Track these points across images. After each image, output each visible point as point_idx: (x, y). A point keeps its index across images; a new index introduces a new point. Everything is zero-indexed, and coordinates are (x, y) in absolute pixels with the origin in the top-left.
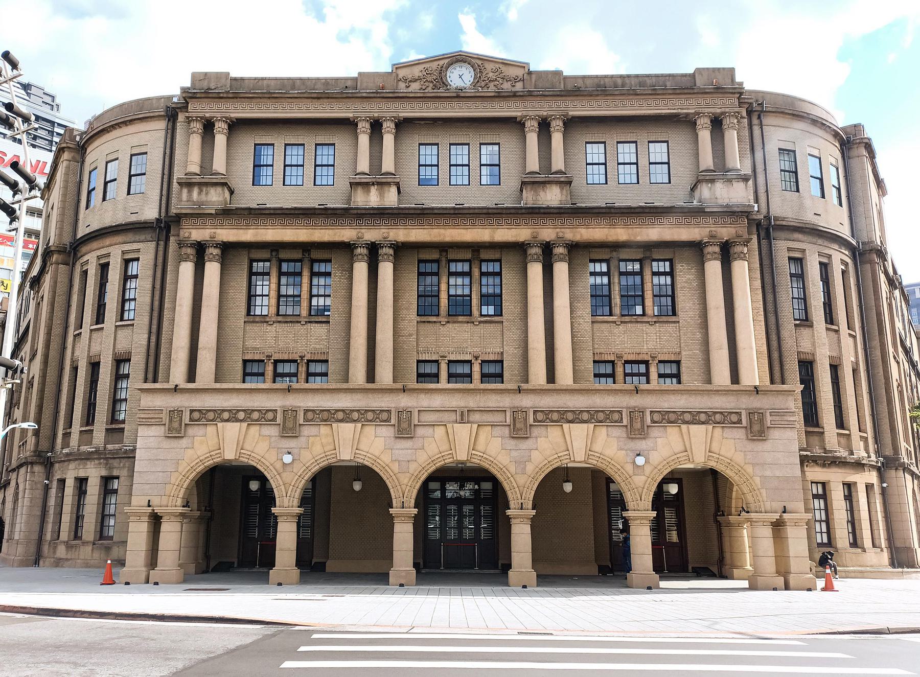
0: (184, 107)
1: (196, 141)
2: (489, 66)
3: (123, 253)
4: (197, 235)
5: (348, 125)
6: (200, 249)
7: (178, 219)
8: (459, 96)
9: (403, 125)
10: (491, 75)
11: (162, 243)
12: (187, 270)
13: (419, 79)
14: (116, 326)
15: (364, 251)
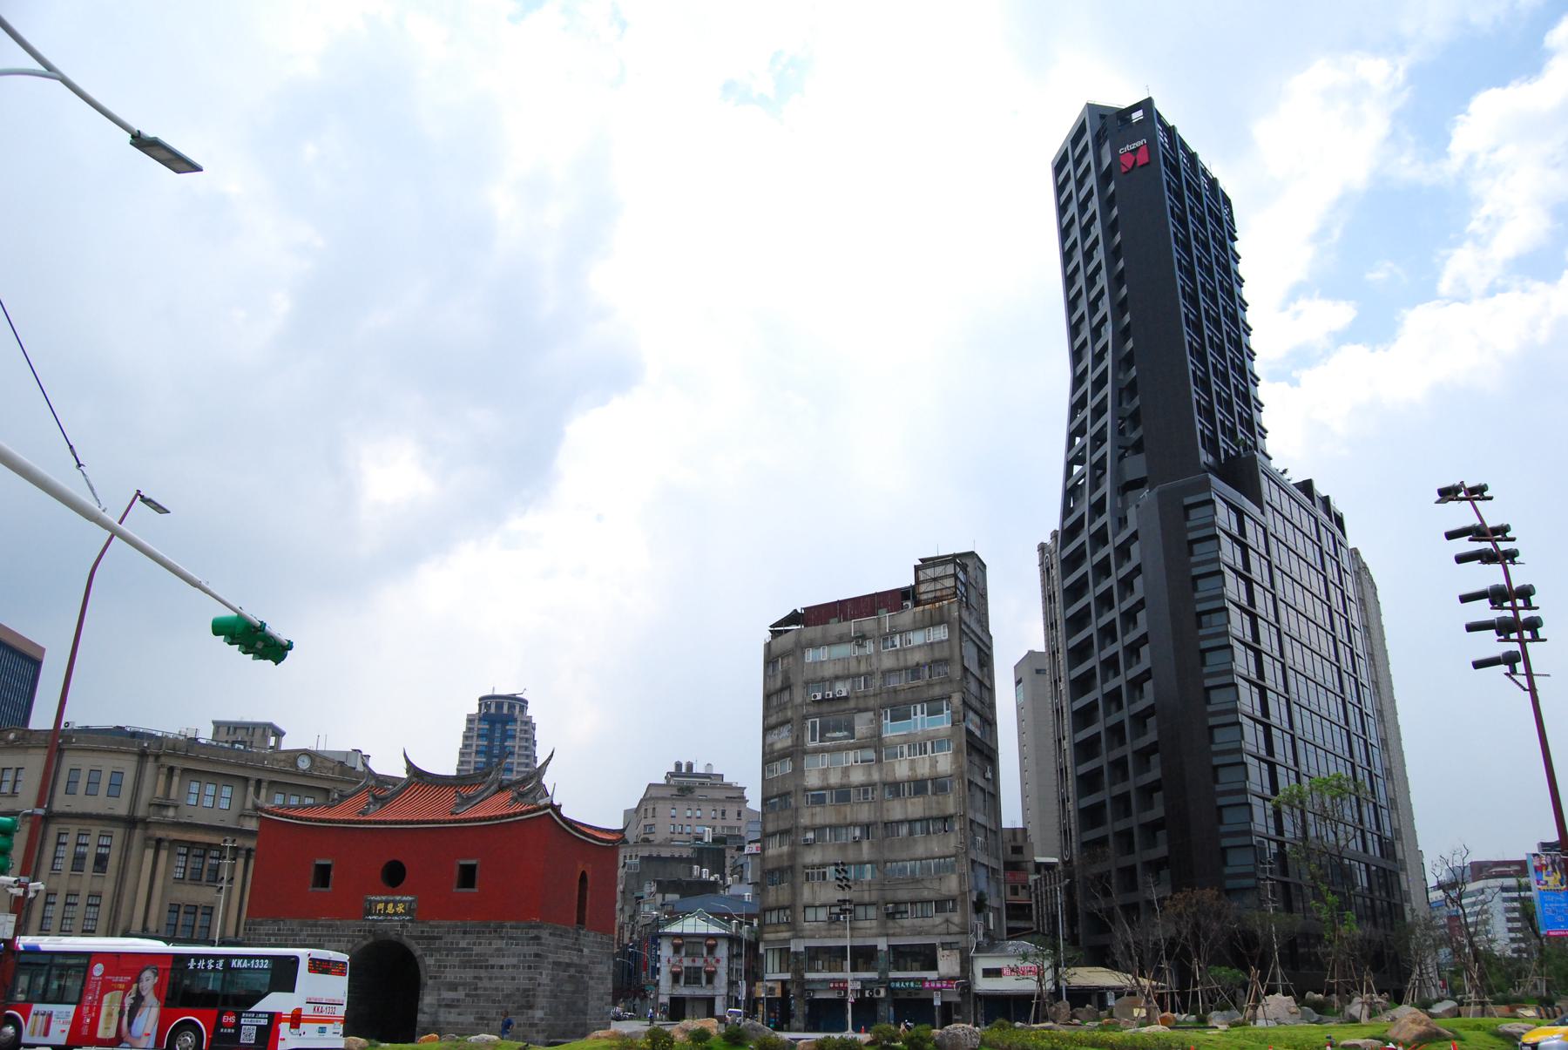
0: (157, 757)
1: (162, 779)
2: (318, 759)
3: (101, 831)
4: (160, 833)
5: (246, 780)
6: (159, 841)
7: (145, 823)
8: (304, 774)
9: (272, 783)
10: (319, 764)
11: (128, 830)
12: (150, 853)
13: (284, 761)
14: (93, 876)
15: (244, 852)
